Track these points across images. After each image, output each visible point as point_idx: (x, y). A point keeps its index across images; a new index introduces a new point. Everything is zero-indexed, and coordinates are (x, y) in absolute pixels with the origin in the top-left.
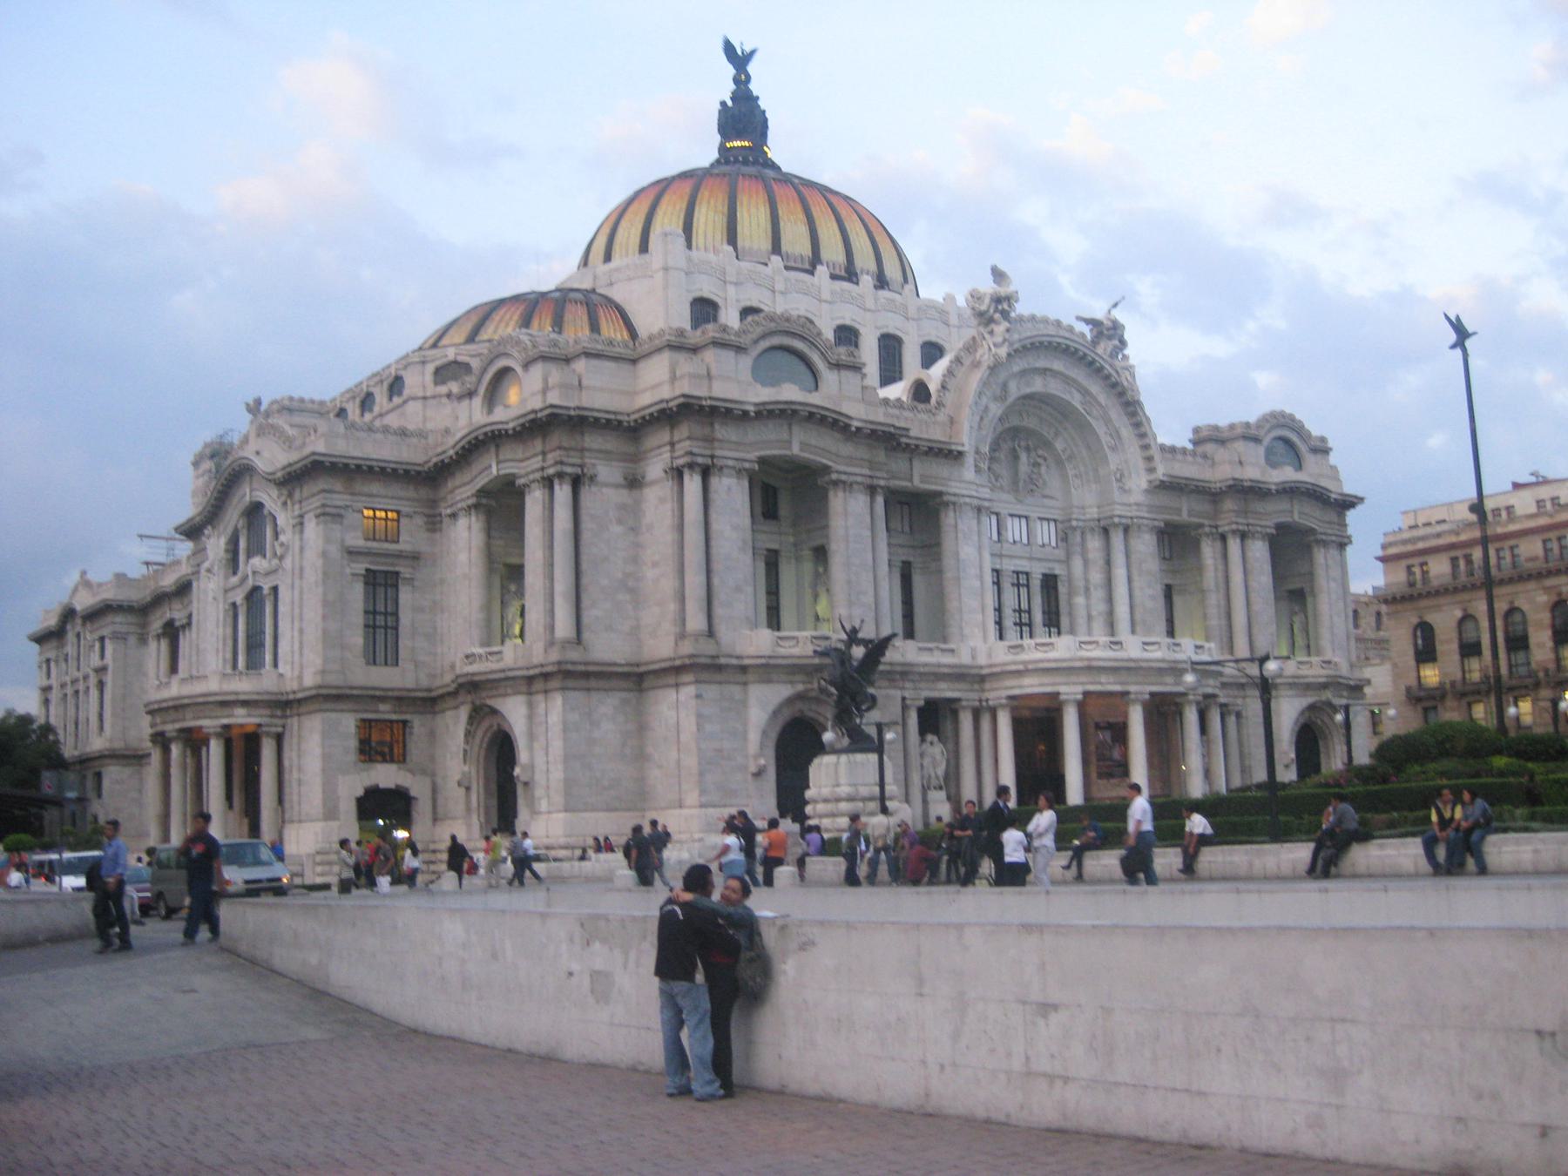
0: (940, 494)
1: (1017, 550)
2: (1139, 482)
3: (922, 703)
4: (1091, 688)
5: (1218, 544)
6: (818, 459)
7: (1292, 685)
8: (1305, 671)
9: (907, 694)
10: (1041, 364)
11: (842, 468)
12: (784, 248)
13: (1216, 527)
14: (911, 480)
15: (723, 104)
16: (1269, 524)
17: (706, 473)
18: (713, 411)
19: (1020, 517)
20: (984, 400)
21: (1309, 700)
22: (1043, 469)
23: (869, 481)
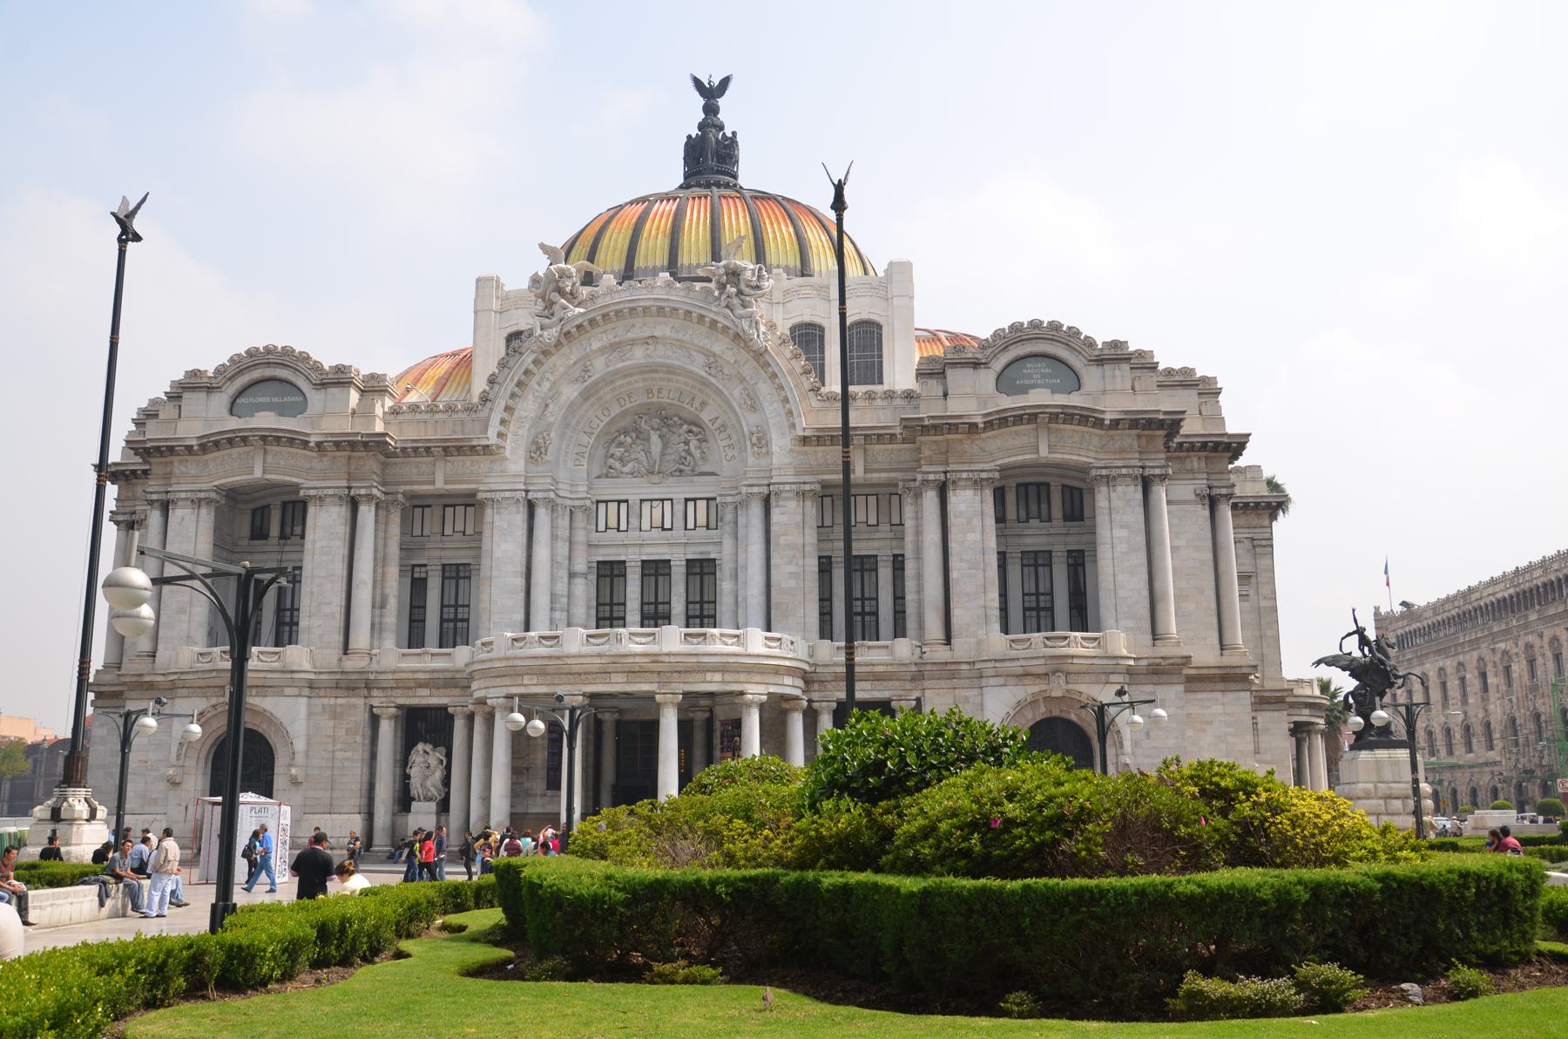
0: (473, 494)
2: (781, 447)
3: (393, 711)
4: (514, 690)
6: (287, 478)
9: (375, 702)
11: (318, 484)
12: (640, 262)
14: (433, 483)
15: (689, 137)
17: (165, 507)
18: (158, 449)
20: (547, 385)
21: (1035, 688)
22: (693, 443)
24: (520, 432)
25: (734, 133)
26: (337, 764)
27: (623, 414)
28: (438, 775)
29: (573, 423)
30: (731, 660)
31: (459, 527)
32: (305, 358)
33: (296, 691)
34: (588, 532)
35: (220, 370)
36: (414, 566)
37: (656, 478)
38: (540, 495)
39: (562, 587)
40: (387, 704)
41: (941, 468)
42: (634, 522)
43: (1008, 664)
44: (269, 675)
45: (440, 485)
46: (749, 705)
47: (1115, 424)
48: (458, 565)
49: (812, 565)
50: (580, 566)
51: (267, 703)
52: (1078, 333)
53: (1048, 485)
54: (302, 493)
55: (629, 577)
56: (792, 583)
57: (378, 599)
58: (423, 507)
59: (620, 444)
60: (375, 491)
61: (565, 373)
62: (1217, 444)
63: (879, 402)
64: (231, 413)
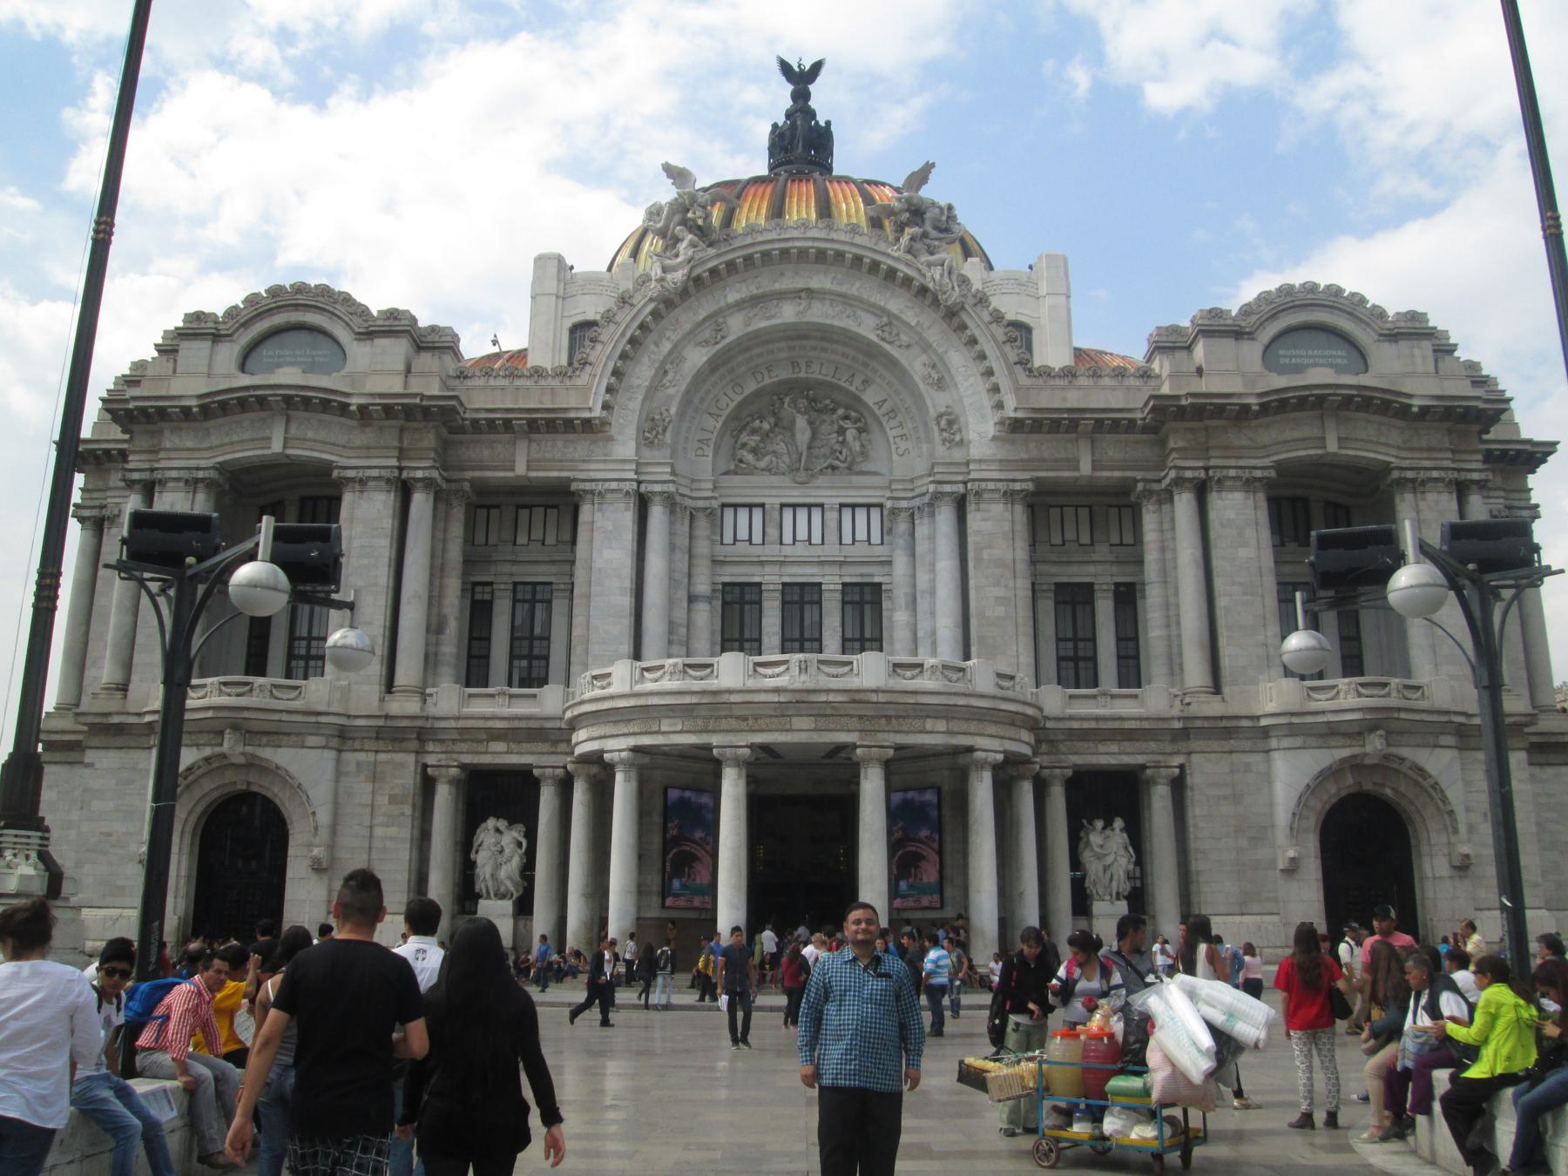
1: (800, 551)
2: (981, 430)
3: (454, 771)
4: (646, 741)
5: (1166, 508)
7: (1292, 730)
8: (1322, 702)
9: (431, 760)
10: (787, 283)
13: (1159, 481)
16: (1262, 464)
19: (809, 506)
22: (851, 434)
23: (386, 473)
24: (631, 405)
25: (828, 123)
26: (377, 844)
27: (756, 395)
28: (515, 864)
29: (696, 401)
30: (962, 701)
31: (537, 534)
32: (347, 299)
33: (321, 741)
34: (713, 542)
35: (232, 312)
36: (475, 584)
37: (802, 476)
38: (657, 488)
39: (680, 614)
40: (447, 762)
41: (1200, 464)
42: (773, 532)
43: (1309, 719)
44: (285, 717)
45: (520, 469)
46: (981, 765)
47: (1425, 410)
48: (535, 584)
49: (1023, 586)
50: (702, 587)
51: (282, 757)
52: (1363, 300)
53: (1305, 500)
54: (335, 474)
55: (766, 604)
56: (1000, 611)
57: (434, 620)
58: (489, 507)
59: (754, 432)
60: (435, 474)
61: (691, 332)
62: (1519, 452)
63: (1107, 381)
64: (243, 368)
